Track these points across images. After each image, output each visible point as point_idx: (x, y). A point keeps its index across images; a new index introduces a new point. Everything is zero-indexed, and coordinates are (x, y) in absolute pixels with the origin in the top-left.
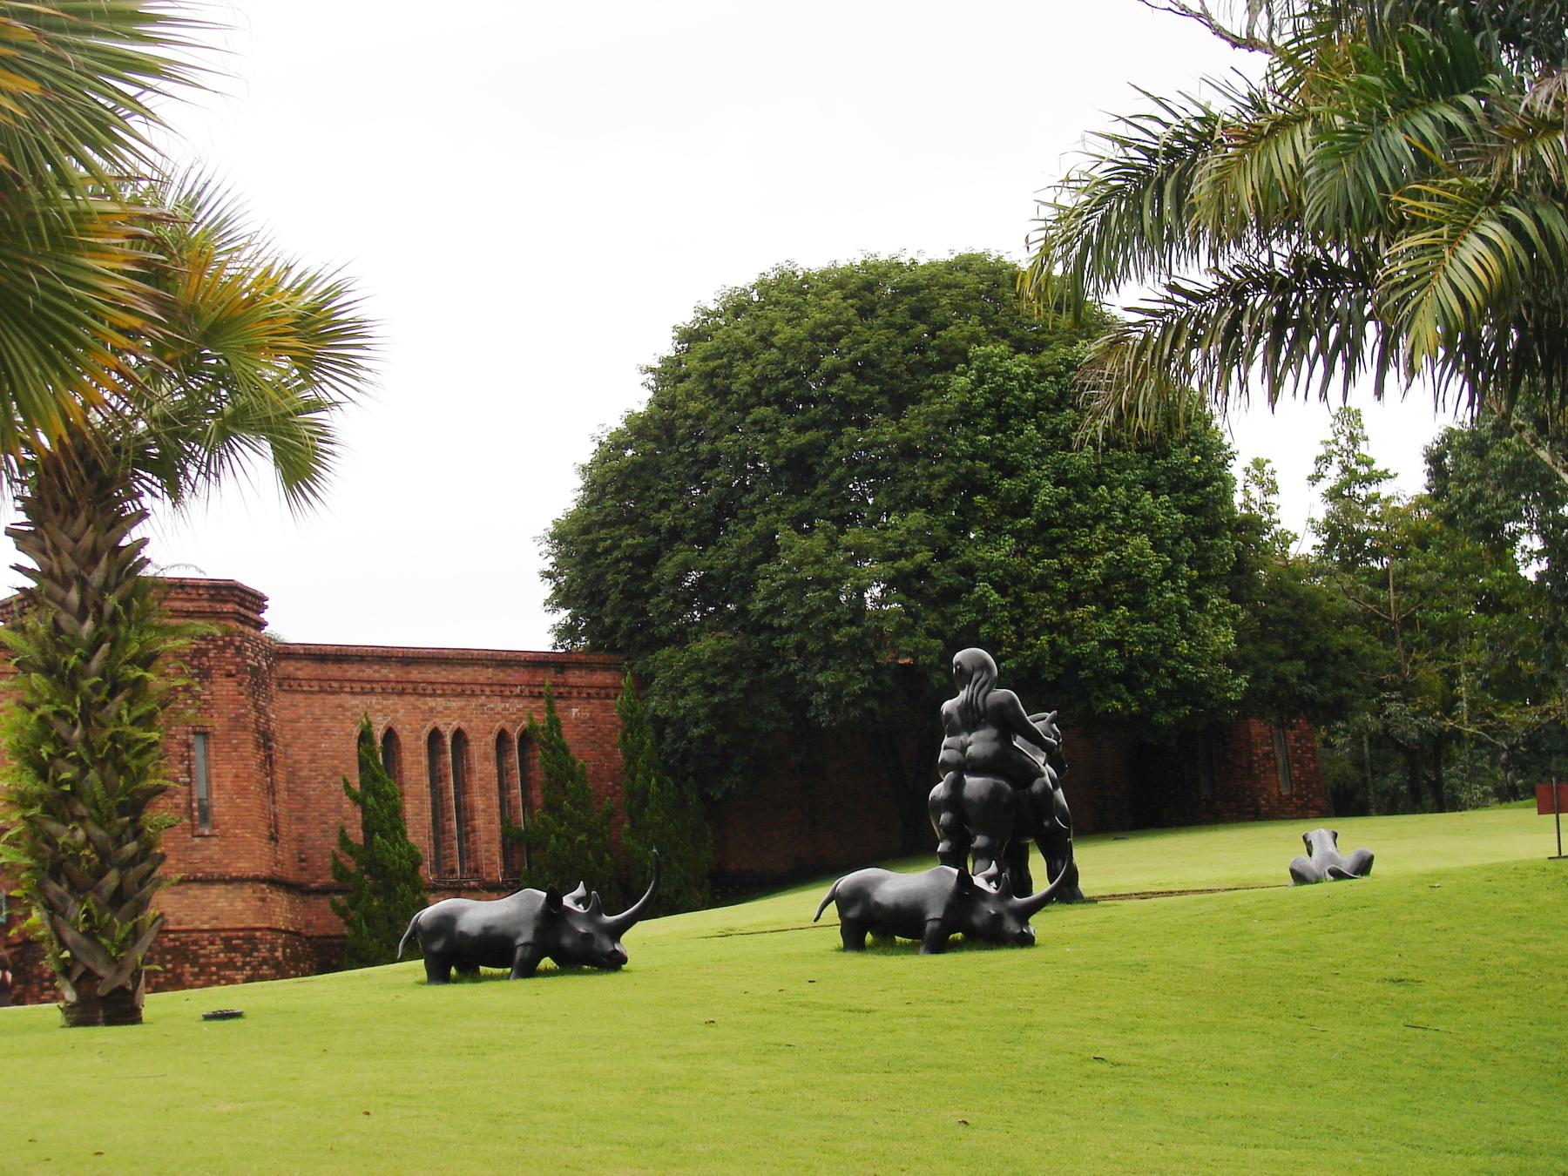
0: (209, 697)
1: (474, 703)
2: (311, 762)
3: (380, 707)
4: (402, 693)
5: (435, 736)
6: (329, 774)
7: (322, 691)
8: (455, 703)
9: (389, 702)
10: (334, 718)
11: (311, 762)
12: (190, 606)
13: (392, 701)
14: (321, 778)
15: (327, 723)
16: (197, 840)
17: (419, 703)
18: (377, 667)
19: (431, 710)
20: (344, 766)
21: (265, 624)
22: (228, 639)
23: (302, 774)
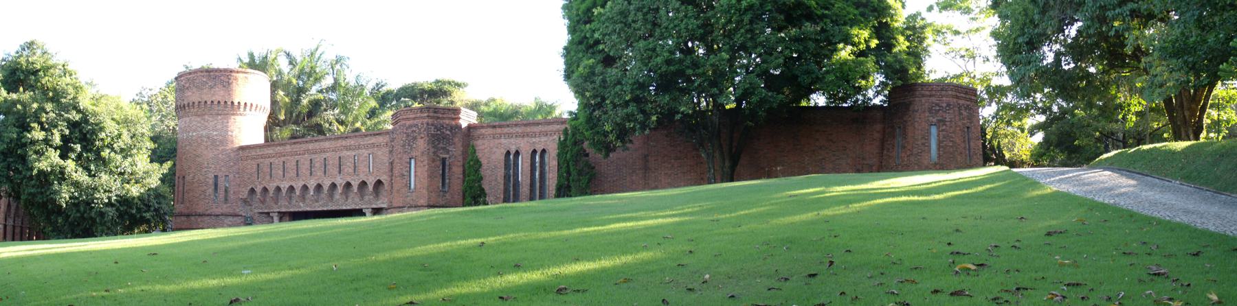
1: (551, 138)
4: (523, 136)
5: (534, 152)
7: (494, 138)
8: (543, 139)
12: (414, 116)
13: (519, 140)
15: (495, 149)
16: (409, 194)
19: (534, 143)
21: (460, 118)
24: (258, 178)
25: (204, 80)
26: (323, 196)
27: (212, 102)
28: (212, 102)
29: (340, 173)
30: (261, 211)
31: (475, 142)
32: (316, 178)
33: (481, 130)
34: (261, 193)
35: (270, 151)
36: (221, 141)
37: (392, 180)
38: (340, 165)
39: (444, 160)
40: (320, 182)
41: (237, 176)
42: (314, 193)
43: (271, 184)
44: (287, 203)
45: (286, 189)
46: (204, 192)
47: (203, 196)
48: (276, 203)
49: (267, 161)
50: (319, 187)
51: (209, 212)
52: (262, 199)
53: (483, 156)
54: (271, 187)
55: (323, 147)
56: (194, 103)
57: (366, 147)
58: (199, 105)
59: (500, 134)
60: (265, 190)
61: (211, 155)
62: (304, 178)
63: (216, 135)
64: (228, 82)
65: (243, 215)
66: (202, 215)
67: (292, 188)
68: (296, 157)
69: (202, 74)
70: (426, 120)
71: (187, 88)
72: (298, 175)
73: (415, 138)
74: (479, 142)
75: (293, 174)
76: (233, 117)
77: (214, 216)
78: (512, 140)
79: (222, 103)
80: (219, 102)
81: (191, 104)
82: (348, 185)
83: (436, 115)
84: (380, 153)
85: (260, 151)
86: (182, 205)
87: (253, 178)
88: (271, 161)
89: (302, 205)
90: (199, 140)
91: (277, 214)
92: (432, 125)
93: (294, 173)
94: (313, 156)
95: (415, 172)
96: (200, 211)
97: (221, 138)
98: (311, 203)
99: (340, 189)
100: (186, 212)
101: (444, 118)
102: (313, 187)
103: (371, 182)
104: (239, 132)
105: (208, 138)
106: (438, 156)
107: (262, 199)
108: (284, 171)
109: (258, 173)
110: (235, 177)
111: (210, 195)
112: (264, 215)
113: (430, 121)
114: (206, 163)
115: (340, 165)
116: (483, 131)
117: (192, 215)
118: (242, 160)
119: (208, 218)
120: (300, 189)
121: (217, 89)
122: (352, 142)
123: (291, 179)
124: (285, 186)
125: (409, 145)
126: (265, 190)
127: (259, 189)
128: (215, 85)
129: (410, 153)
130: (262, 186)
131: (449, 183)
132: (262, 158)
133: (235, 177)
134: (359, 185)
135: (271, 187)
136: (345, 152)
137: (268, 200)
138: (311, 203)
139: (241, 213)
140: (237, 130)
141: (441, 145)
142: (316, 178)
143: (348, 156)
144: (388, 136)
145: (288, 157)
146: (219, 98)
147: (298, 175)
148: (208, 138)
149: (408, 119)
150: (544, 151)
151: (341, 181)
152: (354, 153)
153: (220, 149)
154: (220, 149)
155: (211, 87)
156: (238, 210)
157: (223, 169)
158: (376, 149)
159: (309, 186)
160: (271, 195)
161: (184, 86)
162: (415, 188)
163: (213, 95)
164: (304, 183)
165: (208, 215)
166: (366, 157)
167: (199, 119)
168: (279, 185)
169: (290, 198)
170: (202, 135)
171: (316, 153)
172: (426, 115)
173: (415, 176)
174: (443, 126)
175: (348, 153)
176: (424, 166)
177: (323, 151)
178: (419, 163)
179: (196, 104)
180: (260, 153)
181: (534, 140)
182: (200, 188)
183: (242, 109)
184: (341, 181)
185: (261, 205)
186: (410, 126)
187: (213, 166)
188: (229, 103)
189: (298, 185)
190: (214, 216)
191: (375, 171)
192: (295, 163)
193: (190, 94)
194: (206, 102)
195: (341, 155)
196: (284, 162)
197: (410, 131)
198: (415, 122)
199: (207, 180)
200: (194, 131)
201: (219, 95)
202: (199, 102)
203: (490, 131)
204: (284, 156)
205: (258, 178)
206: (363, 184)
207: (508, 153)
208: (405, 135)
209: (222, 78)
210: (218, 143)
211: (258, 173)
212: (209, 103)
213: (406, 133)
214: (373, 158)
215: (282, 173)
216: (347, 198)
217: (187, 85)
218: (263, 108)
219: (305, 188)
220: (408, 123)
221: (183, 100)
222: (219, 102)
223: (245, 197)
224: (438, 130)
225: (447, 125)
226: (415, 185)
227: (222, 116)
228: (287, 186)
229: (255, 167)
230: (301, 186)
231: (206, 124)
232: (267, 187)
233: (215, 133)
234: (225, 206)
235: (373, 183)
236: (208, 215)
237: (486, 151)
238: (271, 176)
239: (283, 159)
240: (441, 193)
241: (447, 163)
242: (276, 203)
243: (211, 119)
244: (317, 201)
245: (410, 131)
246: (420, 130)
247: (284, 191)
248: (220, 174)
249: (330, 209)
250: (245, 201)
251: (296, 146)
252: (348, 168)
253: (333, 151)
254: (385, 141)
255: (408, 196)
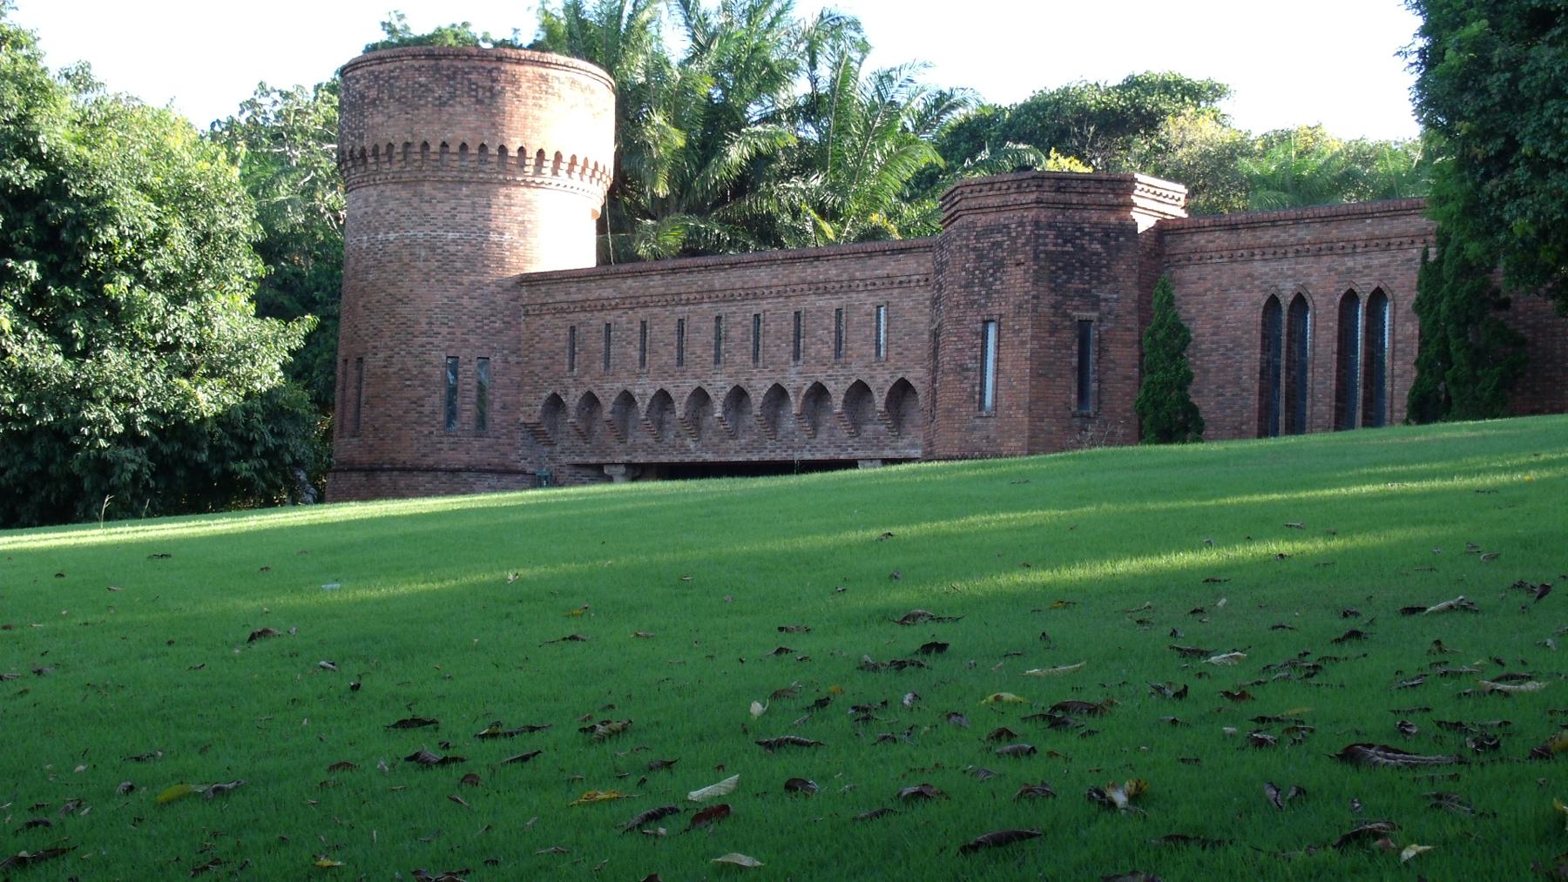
0: (999, 287)
1: (1401, 256)
2: (1214, 334)
3: (1290, 273)
4: (1318, 254)
5: (1350, 298)
6: (1230, 346)
7: (1232, 259)
8: (1379, 259)
9: (1300, 267)
10: (1241, 287)
11: (1214, 334)
12: (997, 201)
14: (1222, 350)
15: (1233, 292)
16: (978, 422)
17: (1335, 265)
18: (1292, 231)
19: (1349, 270)
20: (1246, 336)
21: (1132, 205)
22: (1020, 229)
23: (1203, 347)
24: (572, 367)
25: (422, 80)
26: (750, 420)
27: (444, 145)
28: (444, 145)
29: (796, 357)
30: (578, 460)
31: (1178, 273)
32: (731, 370)
33: (1195, 238)
34: (580, 409)
35: (606, 291)
36: (467, 259)
37: (934, 380)
38: (797, 335)
39: (1083, 327)
40: (742, 382)
41: (513, 359)
42: (725, 413)
43: (607, 386)
44: (650, 440)
45: (648, 401)
46: (418, 402)
47: (413, 416)
48: (622, 439)
49: (597, 320)
50: (738, 396)
51: (430, 461)
52: (582, 426)
53: (1199, 311)
54: (608, 394)
55: (751, 284)
56: (390, 146)
57: (871, 286)
58: (405, 154)
59: (1251, 248)
60: (591, 401)
61: (439, 298)
62: (698, 370)
63: (454, 241)
64: (491, 89)
65: (530, 470)
66: (410, 470)
67: (663, 398)
68: (679, 309)
69: (417, 64)
70: (1031, 215)
71: (373, 102)
72: (680, 361)
73: (999, 265)
74: (1191, 273)
75: (667, 356)
76: (503, 190)
77: (446, 471)
78: (1285, 266)
79: (474, 150)
80: (464, 146)
81: (382, 150)
82: (818, 393)
83: (1060, 197)
84: (907, 304)
85: (579, 291)
86: (355, 441)
87: (557, 368)
88: (609, 318)
89: (692, 446)
90: (405, 252)
91: (622, 469)
92: (1050, 226)
93: (671, 354)
94: (724, 309)
95: (998, 360)
96: (406, 456)
97: (467, 249)
98: (716, 440)
99: (795, 404)
100: (365, 459)
101: (1085, 207)
102: (723, 394)
103: (881, 384)
104: (522, 234)
105: (433, 249)
106: (1066, 316)
107: (582, 426)
108: (643, 350)
109: (573, 354)
110: (506, 361)
111: (434, 412)
112: (589, 472)
113: (1044, 215)
114: (424, 320)
115: (797, 335)
116: (1201, 240)
117: (383, 470)
118: (527, 314)
119: (428, 477)
120: (685, 398)
121: (459, 109)
122: (834, 272)
123: (662, 372)
124: (644, 390)
125: (982, 284)
126: (591, 401)
127: (572, 399)
128: (453, 96)
129: (985, 306)
130: (581, 392)
131: (1099, 391)
132: (583, 310)
133: (506, 361)
134: (848, 393)
135: (608, 394)
136: (813, 297)
137: (598, 429)
138: (716, 440)
139: (522, 464)
140: (515, 229)
141: (1076, 284)
142: (731, 370)
143: (820, 310)
144: (930, 256)
145: (656, 310)
146: (466, 136)
147: (680, 361)
148: (433, 249)
149: (980, 209)
150: (1378, 297)
151: (800, 381)
152: (835, 303)
153: (466, 280)
154: (466, 280)
155: (442, 104)
156: (513, 457)
157: (472, 339)
158: (896, 292)
159: (711, 394)
160: (606, 415)
161: (363, 97)
162: (995, 407)
163: (449, 124)
164: (696, 383)
165: (429, 470)
166: (870, 314)
167: (404, 194)
168: (630, 388)
169: (660, 424)
170: (414, 240)
171: (730, 300)
172: (1033, 197)
173: (997, 371)
174: (1081, 229)
175: (821, 303)
176: (1023, 343)
177: (752, 294)
178: (1008, 335)
179: (399, 149)
180: (580, 297)
181: (1350, 264)
182: (408, 393)
183: (530, 170)
184: (800, 381)
185: (580, 443)
186: (989, 230)
187: (445, 330)
188: (493, 150)
189: (681, 390)
190: (446, 471)
191: (892, 353)
192: (673, 328)
193: (379, 119)
194: (425, 145)
195: (802, 307)
196: (643, 324)
197: (985, 244)
198: (1003, 218)
199: (427, 369)
200: (392, 227)
201: (463, 125)
202: (407, 145)
203: (1222, 239)
204: (645, 305)
205: (572, 367)
206: (860, 391)
207: (1273, 303)
208: (972, 256)
209: (473, 77)
210: (458, 265)
211: (573, 354)
212: (434, 147)
213: (975, 249)
214: (888, 319)
215: (636, 354)
216: (815, 428)
217: (373, 93)
218: (591, 166)
219: (700, 397)
220: (982, 220)
221: (361, 137)
222: (464, 146)
223: (535, 419)
224: (1066, 242)
225: (1095, 225)
226: (996, 396)
227: (472, 186)
228: (652, 392)
229: (564, 334)
230: (690, 391)
231: (426, 208)
232: (596, 392)
233: (451, 235)
234: (477, 444)
235: (887, 389)
236: (429, 470)
237: (1209, 297)
238: (607, 366)
239: (641, 313)
240: (1077, 421)
241: (1094, 334)
242: (622, 439)
243: (440, 195)
244: (733, 436)
245: (985, 244)
246: (1014, 240)
247: (642, 406)
248: (464, 354)
249: (767, 458)
250: (534, 431)
251: (677, 278)
252: (819, 344)
253: (779, 294)
254: (922, 270)
255: (974, 429)
